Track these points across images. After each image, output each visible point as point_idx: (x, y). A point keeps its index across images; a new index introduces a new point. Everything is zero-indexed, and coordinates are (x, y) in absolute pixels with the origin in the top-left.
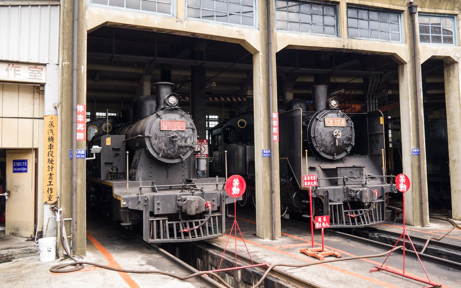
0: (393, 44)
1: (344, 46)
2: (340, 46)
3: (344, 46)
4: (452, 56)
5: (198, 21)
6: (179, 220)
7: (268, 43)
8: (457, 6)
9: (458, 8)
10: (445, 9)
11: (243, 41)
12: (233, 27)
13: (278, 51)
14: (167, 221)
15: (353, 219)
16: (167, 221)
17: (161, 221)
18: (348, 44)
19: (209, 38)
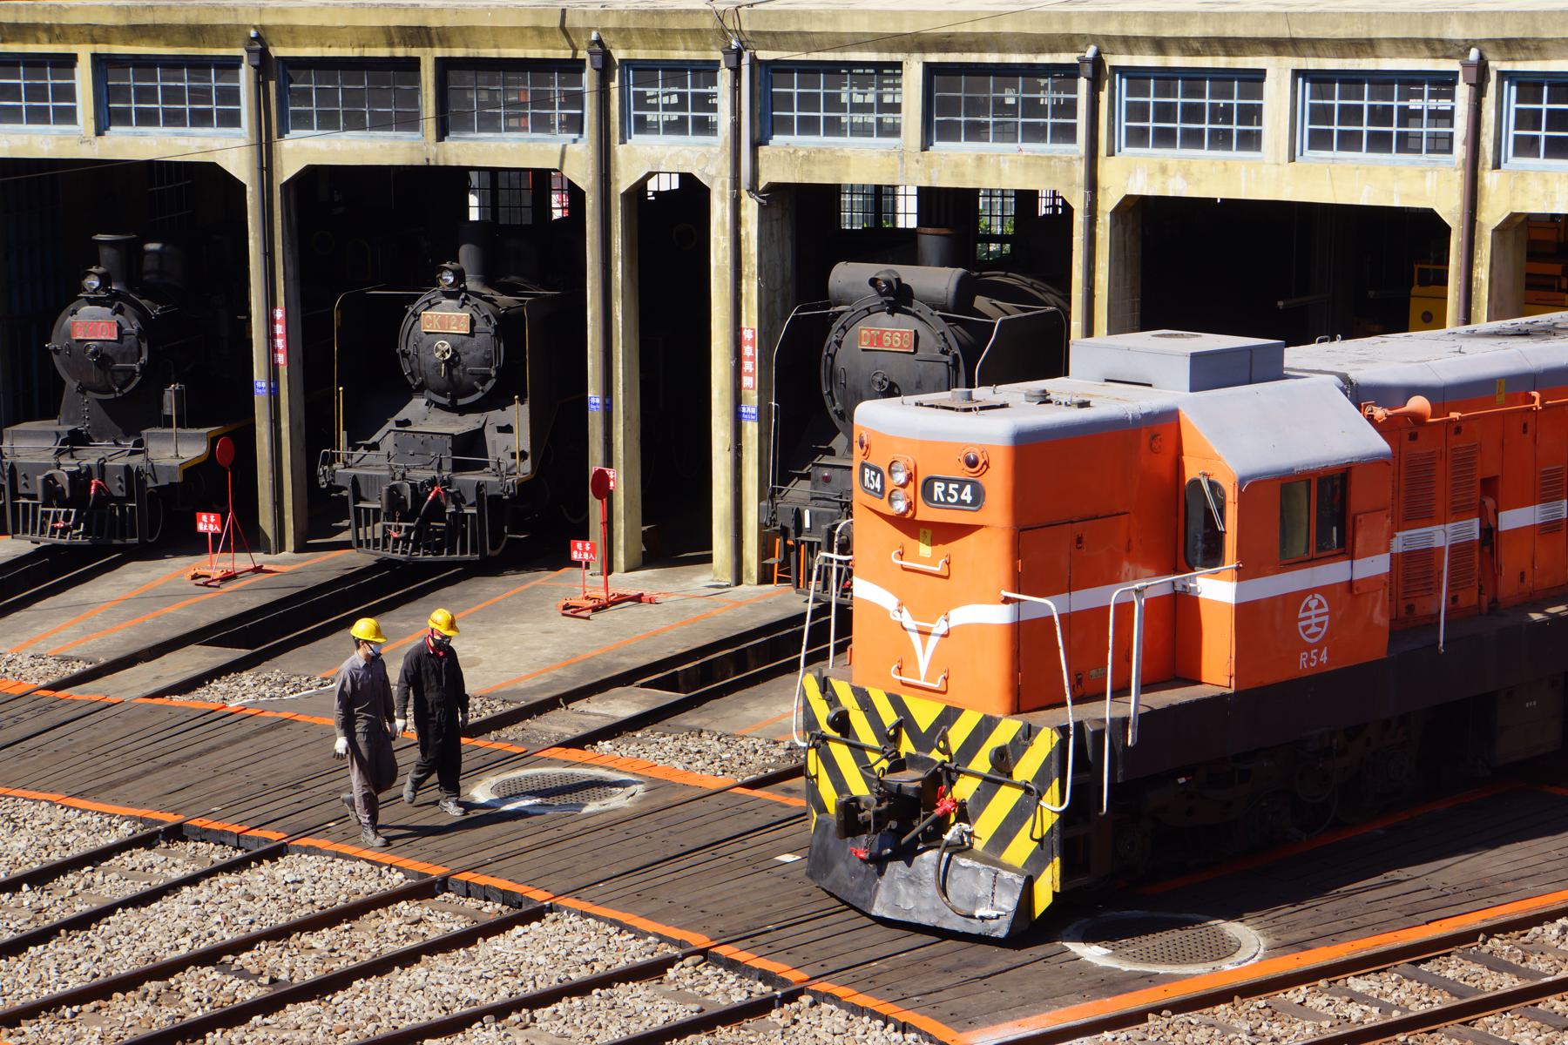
4: (697, 175)
5: (127, 133)
7: (266, 166)
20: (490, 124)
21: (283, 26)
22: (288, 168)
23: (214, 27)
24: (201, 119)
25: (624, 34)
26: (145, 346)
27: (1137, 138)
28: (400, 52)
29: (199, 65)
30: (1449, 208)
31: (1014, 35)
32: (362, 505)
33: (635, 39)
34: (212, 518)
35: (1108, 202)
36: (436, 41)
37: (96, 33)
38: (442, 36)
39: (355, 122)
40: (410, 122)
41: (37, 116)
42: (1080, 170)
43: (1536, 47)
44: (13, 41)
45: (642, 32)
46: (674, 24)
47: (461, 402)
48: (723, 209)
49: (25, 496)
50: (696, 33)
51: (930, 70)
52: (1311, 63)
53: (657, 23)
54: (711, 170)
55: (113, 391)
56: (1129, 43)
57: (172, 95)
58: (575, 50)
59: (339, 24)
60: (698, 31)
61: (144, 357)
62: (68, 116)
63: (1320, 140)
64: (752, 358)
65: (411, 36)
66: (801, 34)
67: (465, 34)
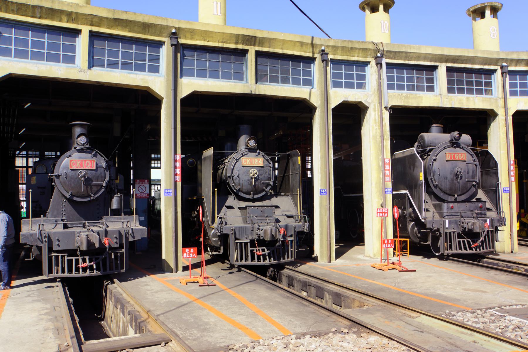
0: (303, 89)
1: (251, 91)
2: (247, 91)
3: (251, 91)
4: (363, 102)
5: (103, 70)
6: (78, 256)
8: (369, 53)
9: (370, 55)
10: (358, 57)
11: (148, 88)
12: (137, 75)
13: (183, 96)
14: (66, 257)
15: (259, 257)
16: (66, 257)
17: (60, 257)
18: (255, 90)
19: (114, 86)
21: (190, 29)
22: (185, 91)
23: (156, 25)
24: (140, 68)
25: (335, 48)
26: (107, 173)
28: (240, 47)
31: (481, 58)
32: (237, 241)
33: (339, 51)
34: (192, 250)
35: (511, 112)
36: (257, 44)
37: (95, 20)
38: (261, 41)
39: (214, 75)
42: (501, 102)
44: (46, 18)
45: (343, 48)
46: (357, 46)
47: (256, 197)
48: (375, 115)
49: (57, 252)
50: (365, 50)
51: (449, 70)
53: (350, 45)
54: (369, 100)
55: (90, 196)
58: (313, 53)
59: (216, 31)
60: (366, 49)
61: (107, 179)
62: (71, 60)
64: (389, 170)
65: (248, 40)
66: (406, 53)
67: (271, 41)
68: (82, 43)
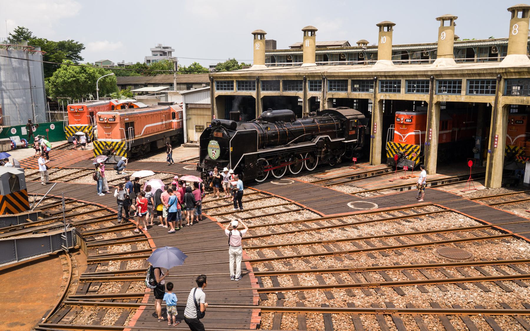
20: (290, 90)
22: (262, 96)
24: (250, 89)
27: (382, 91)
29: (250, 82)
30: (428, 100)
39: (271, 90)
40: (279, 90)
41: (228, 89)
43: (441, 75)
50: (319, 76)
52: (408, 79)
56: (381, 76)
57: (246, 86)
62: (232, 89)
63: (409, 91)
68: (235, 84)
